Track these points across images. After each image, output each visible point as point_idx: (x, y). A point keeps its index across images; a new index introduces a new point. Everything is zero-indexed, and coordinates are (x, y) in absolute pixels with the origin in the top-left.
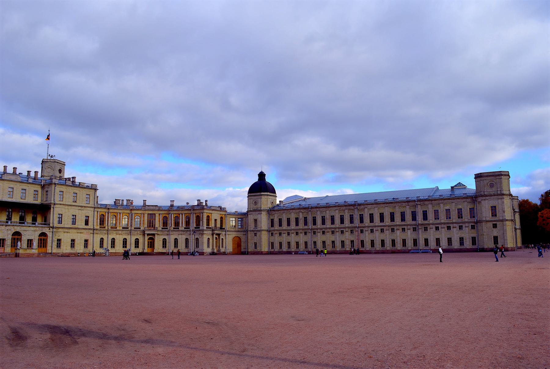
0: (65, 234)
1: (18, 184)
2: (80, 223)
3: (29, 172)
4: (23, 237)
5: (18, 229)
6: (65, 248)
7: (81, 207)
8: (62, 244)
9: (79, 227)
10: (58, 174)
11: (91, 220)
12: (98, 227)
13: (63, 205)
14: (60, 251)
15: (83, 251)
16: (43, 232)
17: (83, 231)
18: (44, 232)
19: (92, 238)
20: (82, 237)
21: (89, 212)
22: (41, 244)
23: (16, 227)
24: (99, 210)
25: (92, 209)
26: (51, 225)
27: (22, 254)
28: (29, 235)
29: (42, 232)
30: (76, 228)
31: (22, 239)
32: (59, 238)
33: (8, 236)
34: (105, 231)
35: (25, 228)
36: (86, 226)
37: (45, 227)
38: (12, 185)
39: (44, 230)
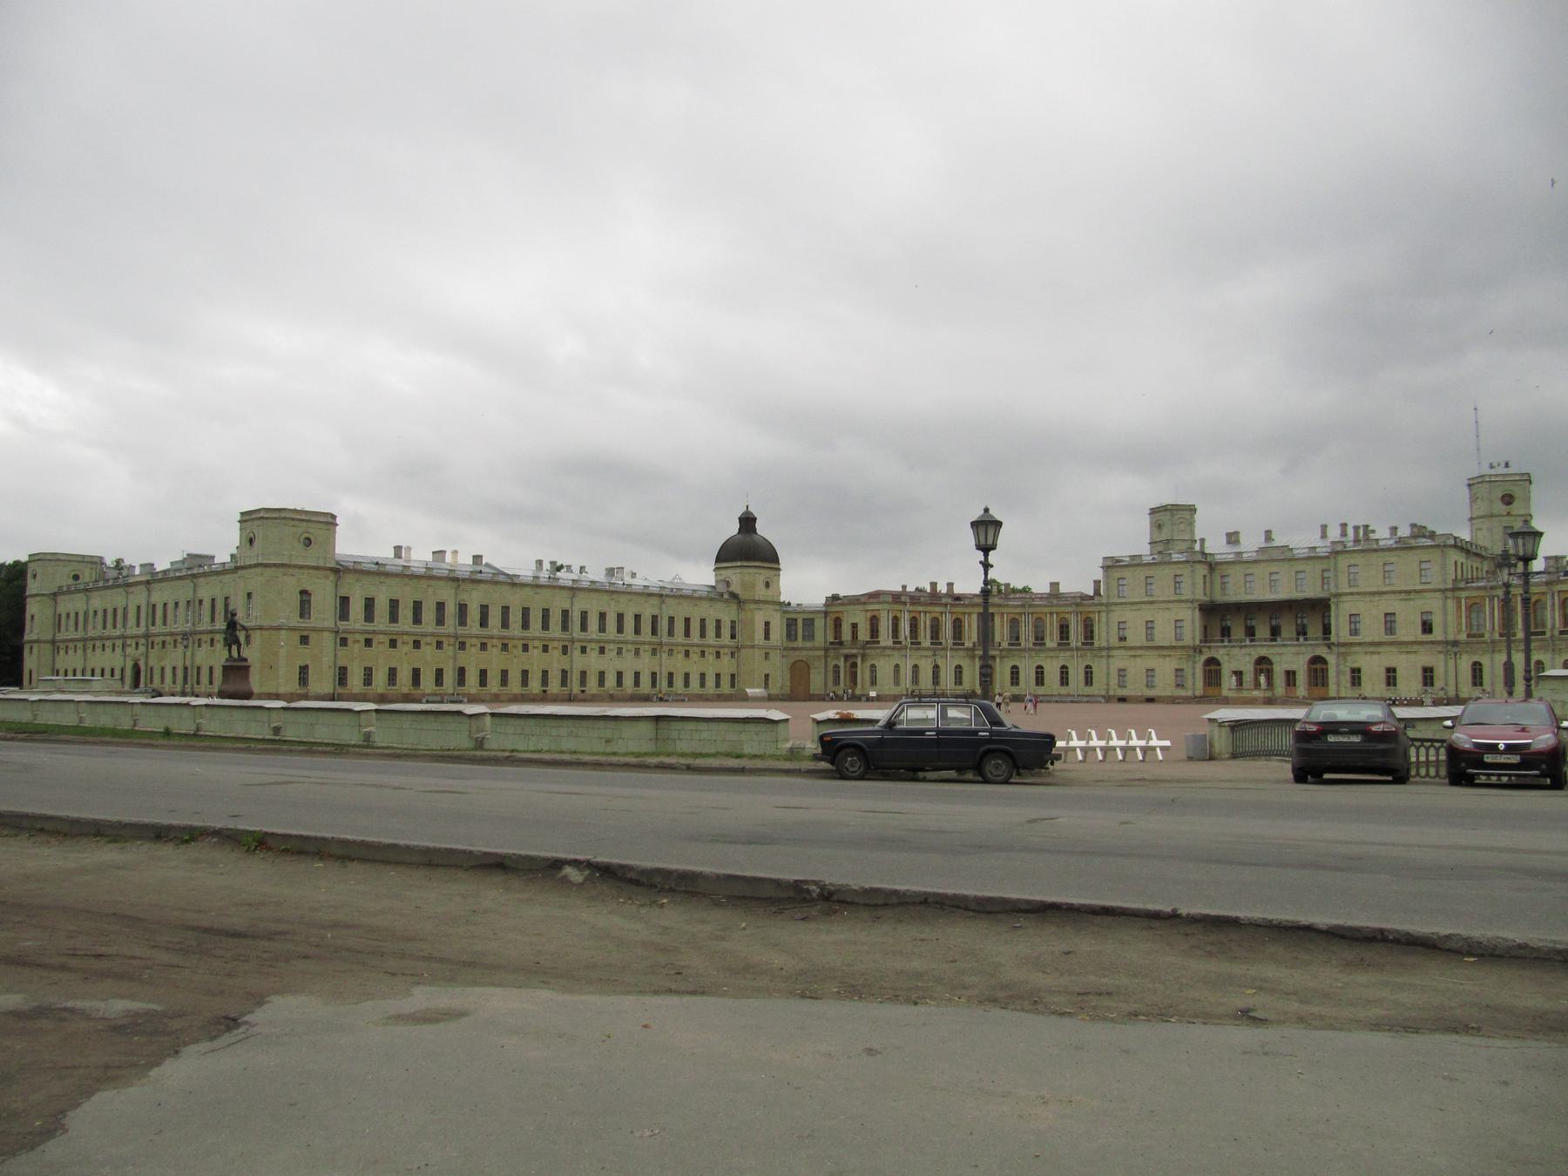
0: (1368, 657)
1: (1286, 566)
2: (1409, 630)
3: (934, 585)
4: (1274, 666)
5: (1263, 652)
8: (1363, 679)
10: (1500, 508)
11: (1437, 621)
12: (1463, 637)
13: (1358, 594)
15: (1418, 694)
17: (1415, 648)
19: (1442, 664)
21: (1433, 604)
23: (1259, 649)
24: (1463, 594)
25: (1438, 595)
28: (1287, 663)
30: (1392, 643)
32: (1356, 665)
34: (1484, 645)
35: (1277, 649)
36: (1424, 636)
37: (1317, 645)
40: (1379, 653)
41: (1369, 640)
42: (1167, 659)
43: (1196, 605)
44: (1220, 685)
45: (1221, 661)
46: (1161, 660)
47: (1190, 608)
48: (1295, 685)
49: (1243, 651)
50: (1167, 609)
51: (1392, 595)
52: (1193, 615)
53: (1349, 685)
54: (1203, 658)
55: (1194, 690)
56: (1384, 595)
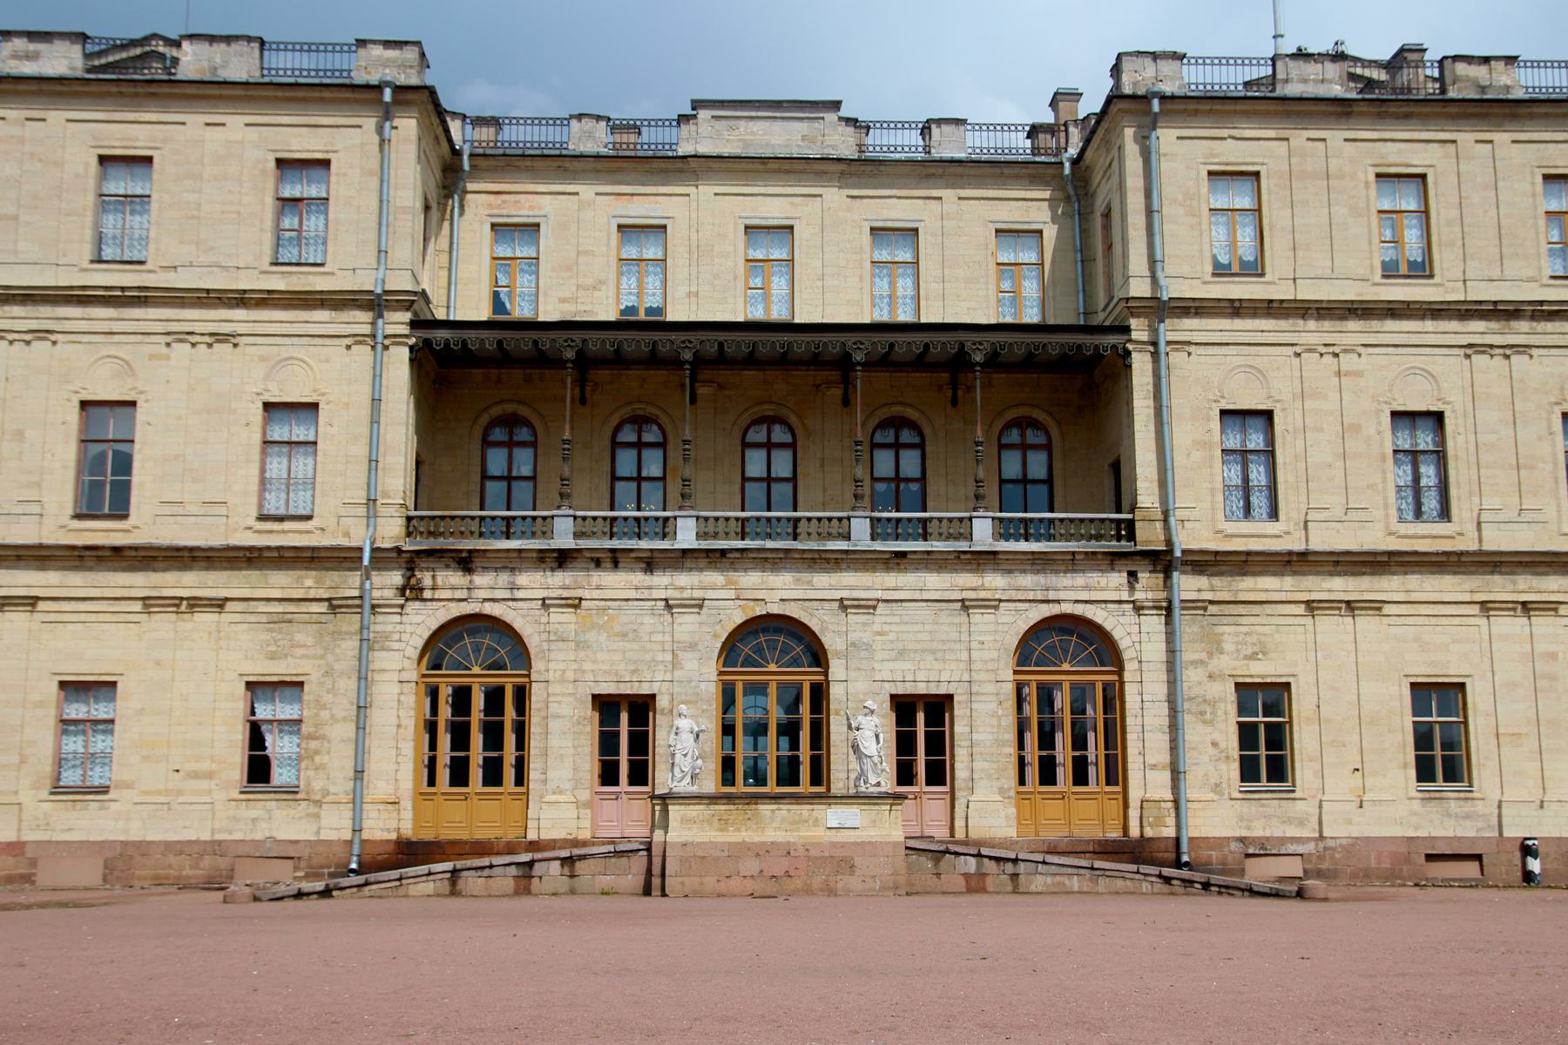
0: (1332, 627)
1: (834, 196)
4: (836, 670)
6: (1340, 785)
7: (1493, 325)
8: (1304, 741)
9: (1498, 540)
13: (1270, 309)
14: (1288, 821)
16: (1055, 610)
18: (1067, 608)
20: (1553, 656)
22: (1047, 740)
23: (752, 579)
26: (1149, 536)
27: (699, 858)
28: (901, 655)
29: (1046, 611)
31: (836, 691)
32: (1262, 670)
33: (675, 664)
38: (771, 203)
39: (1073, 595)
40: (1376, 607)
41: (1323, 540)
42: (206, 619)
43: (397, 322)
44: (520, 780)
45: (533, 641)
46: (163, 624)
47: (359, 339)
48: (938, 774)
49: (664, 582)
50: (220, 338)
51: (1429, 325)
52: (377, 377)
53: (1234, 770)
54: (423, 620)
55: (357, 802)
56: (1391, 325)
